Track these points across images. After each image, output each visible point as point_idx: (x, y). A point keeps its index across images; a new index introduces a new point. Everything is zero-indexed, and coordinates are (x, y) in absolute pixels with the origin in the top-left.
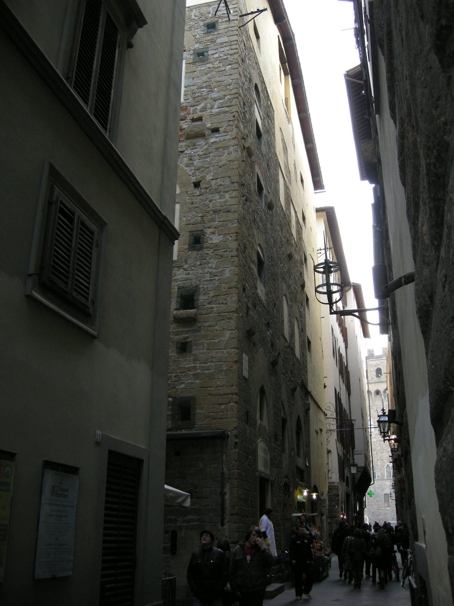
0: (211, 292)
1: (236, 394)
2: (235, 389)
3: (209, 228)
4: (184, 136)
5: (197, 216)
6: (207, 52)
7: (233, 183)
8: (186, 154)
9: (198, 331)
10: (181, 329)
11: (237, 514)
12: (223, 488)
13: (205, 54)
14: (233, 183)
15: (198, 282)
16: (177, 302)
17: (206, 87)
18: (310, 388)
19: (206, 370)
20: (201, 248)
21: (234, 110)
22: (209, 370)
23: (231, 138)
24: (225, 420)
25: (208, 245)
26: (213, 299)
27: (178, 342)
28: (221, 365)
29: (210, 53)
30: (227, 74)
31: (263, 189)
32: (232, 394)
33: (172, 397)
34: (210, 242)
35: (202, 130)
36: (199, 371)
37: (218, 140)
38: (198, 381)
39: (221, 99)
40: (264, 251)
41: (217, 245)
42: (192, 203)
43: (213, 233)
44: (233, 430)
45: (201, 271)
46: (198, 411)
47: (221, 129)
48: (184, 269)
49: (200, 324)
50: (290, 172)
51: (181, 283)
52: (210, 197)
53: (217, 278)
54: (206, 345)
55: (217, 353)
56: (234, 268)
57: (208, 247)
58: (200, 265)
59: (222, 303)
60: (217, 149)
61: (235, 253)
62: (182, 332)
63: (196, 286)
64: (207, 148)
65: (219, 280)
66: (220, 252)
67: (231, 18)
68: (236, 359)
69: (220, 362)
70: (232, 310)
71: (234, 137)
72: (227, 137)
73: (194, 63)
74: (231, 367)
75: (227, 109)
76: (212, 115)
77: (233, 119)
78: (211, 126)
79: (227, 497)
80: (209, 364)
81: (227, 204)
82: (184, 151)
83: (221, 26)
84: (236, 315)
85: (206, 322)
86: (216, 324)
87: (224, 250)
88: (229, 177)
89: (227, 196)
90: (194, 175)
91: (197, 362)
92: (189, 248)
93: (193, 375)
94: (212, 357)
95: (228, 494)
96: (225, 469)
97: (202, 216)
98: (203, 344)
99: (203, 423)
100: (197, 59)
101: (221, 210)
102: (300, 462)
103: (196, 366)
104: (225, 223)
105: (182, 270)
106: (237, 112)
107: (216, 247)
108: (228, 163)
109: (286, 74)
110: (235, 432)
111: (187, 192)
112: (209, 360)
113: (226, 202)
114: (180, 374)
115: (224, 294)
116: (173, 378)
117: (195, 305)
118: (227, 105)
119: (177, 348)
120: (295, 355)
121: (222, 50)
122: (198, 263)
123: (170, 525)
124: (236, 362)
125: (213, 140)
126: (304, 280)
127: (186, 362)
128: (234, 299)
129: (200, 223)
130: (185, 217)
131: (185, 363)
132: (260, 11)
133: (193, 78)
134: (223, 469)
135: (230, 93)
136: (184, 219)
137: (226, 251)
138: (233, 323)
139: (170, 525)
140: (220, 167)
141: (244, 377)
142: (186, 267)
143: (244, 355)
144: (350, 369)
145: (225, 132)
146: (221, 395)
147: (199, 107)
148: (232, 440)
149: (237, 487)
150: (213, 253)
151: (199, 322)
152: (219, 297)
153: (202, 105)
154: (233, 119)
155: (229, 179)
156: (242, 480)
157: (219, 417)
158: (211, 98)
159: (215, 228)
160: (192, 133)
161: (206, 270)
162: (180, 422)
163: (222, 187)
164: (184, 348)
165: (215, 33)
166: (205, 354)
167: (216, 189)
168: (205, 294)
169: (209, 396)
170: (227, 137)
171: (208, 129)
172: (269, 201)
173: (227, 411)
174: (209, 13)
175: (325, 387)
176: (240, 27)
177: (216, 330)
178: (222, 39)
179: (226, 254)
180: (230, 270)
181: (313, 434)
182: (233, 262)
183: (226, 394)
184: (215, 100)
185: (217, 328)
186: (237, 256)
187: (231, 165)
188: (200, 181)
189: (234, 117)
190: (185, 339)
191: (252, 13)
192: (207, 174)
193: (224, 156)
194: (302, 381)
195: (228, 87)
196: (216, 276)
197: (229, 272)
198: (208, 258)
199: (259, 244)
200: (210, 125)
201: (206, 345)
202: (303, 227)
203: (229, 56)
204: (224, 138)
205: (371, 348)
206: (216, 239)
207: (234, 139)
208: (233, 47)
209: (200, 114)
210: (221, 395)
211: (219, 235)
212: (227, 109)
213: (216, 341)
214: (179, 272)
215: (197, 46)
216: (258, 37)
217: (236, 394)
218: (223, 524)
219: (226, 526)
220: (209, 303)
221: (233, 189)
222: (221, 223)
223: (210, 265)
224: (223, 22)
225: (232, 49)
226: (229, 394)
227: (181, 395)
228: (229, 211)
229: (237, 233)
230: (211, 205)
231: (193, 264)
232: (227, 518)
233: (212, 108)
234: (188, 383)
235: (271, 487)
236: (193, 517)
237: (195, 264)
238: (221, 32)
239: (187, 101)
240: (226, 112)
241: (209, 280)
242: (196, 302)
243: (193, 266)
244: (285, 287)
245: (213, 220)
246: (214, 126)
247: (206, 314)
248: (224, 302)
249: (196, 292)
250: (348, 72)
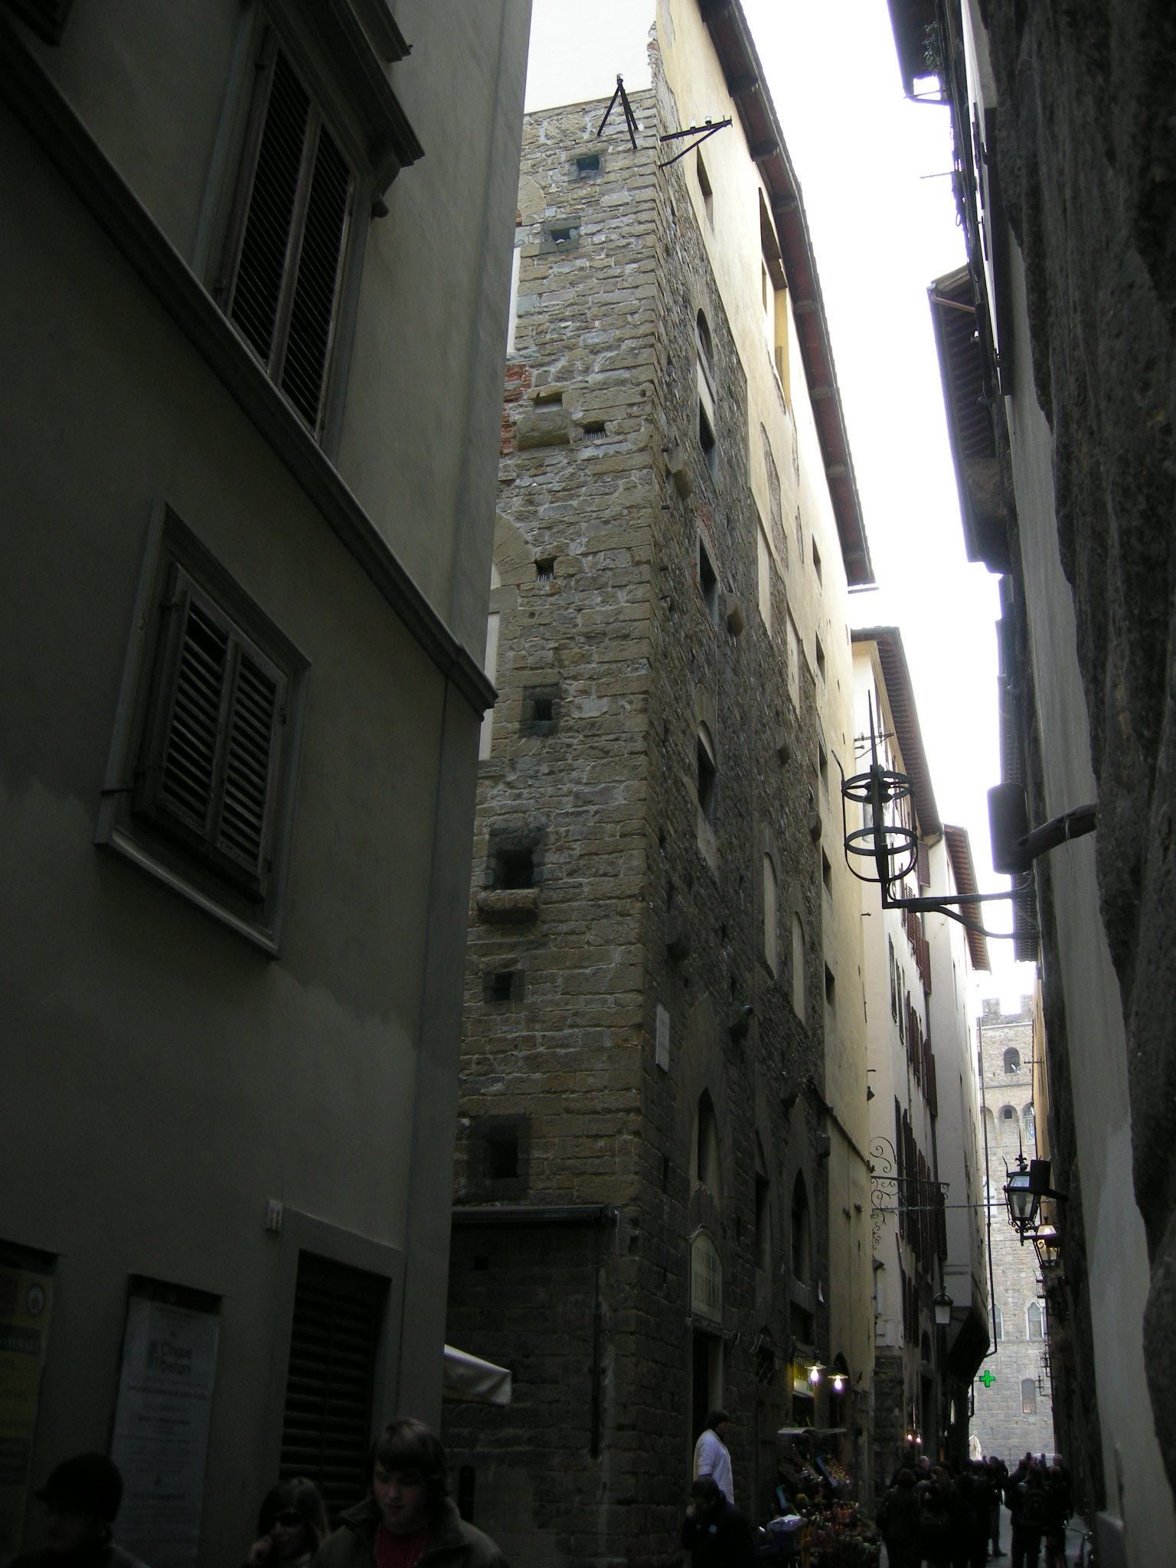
0: (576, 845)
1: (638, 1111)
2: (633, 1098)
3: (574, 678)
4: (514, 443)
5: (543, 648)
6: (576, 228)
7: (638, 564)
8: (519, 487)
9: (543, 945)
10: (497, 940)
11: (634, 1428)
12: (598, 1354)
13: (573, 233)
14: (638, 564)
15: (544, 819)
16: (488, 868)
17: (573, 318)
18: (831, 1098)
19: (562, 1046)
20: (553, 731)
21: (643, 378)
22: (568, 1046)
23: (635, 448)
24: (606, 1178)
25: (571, 722)
26: (582, 862)
27: (487, 974)
28: (600, 1034)
29: (583, 230)
30: (626, 285)
31: (715, 579)
32: (628, 1111)
33: (470, 1117)
34: (576, 715)
35: (560, 429)
36: (541, 1049)
37: (600, 453)
38: (538, 1075)
39: (610, 348)
40: (716, 740)
41: (593, 724)
42: (532, 615)
43: (585, 692)
44: (626, 1205)
45: (550, 790)
46: (537, 1154)
47: (608, 426)
48: (509, 785)
49: (546, 927)
50: (785, 537)
51: (498, 821)
52: (577, 598)
53: (593, 808)
54: (560, 981)
55: (588, 1003)
56: (636, 783)
57: (570, 729)
58: (551, 773)
59: (605, 875)
60: (598, 476)
61: (639, 745)
62: (500, 945)
63: (539, 829)
64: (572, 474)
65: (597, 812)
66: (602, 742)
67: (639, 142)
68: (638, 1020)
69: (597, 1026)
70: (629, 893)
71: (642, 445)
72: (624, 447)
73: (541, 256)
74: (626, 1041)
75: (626, 375)
76: (587, 389)
77: (639, 399)
78: (583, 418)
79: (608, 1381)
80: (567, 1031)
81: (621, 617)
82: (513, 480)
83: (615, 164)
84: (639, 904)
85: (561, 922)
86: (589, 928)
87: (612, 737)
88: (629, 549)
89: (622, 596)
90: (537, 542)
91: (537, 1026)
92: (520, 730)
93: (527, 1058)
94: (576, 1014)
95: (610, 1373)
96: (605, 1308)
97: (556, 649)
98: (553, 979)
99: (548, 1184)
100: (551, 246)
101: (605, 634)
102: (802, 1291)
103: (534, 1036)
104: (614, 666)
105: (501, 786)
106: (652, 382)
107: (591, 728)
108: (625, 512)
109: (778, 287)
110: (632, 1211)
111: (518, 586)
112: (569, 1021)
113: (619, 612)
114: (491, 1057)
115: (610, 849)
116: (474, 1066)
117: (536, 877)
118: (625, 363)
119: (485, 988)
120: (792, 1011)
121: (615, 223)
122: (545, 769)
123: (456, 1450)
124: (639, 1027)
125: (587, 453)
126: (818, 816)
127: (509, 1026)
128: (635, 863)
129: (553, 666)
130: (512, 649)
131: (505, 1028)
132: (712, 127)
133: (540, 295)
134: (598, 1305)
135: (634, 332)
136: (511, 654)
137: (617, 739)
138: (631, 927)
139: (456, 1450)
140: (606, 522)
142: (511, 777)
143: (660, 1009)
144: (934, 1051)
145: (619, 434)
146: (598, 1113)
147: (553, 369)
148: (623, 1232)
149: (633, 1355)
150: (582, 742)
151: (545, 922)
152: (597, 858)
153: (562, 363)
154: (639, 399)
155: (628, 555)
158: (586, 347)
159: (591, 678)
160: (536, 434)
161: (565, 789)
162: (488, 1182)
163: (610, 573)
164: (503, 988)
165: (599, 181)
166: (558, 1004)
167: (594, 579)
168: (560, 849)
169: (565, 1116)
170: (624, 447)
171: (577, 424)
172: (729, 612)
174: (584, 129)
175: (870, 1095)
176: (661, 166)
177: (588, 943)
178: (615, 196)
179: (616, 745)
180: (627, 789)
181: (836, 1219)
182: (635, 768)
183: (609, 1111)
184: (595, 351)
185: (589, 937)
186: (645, 753)
187: (633, 519)
188: (555, 558)
189: (643, 394)
190: (506, 966)
191: (694, 130)
192: (572, 540)
193: (616, 494)
194: (810, 1080)
195: (629, 318)
196: (590, 802)
197: (625, 793)
198: (570, 757)
199: (703, 723)
200: (581, 414)
201: (560, 981)
202: (818, 681)
203: (632, 240)
204: (617, 447)
205: (991, 996)
206: (592, 708)
207: (642, 450)
208: (644, 216)
209: (555, 386)
210: (598, 1113)
211: (599, 697)
212: (626, 375)
213: (588, 971)
214: (495, 792)
215: (550, 213)
216: (707, 191)
217: (638, 1111)
218: (595, 1452)
219: (605, 1458)
220: (570, 874)
221: (638, 578)
222: (606, 666)
223: (574, 774)
224: (619, 153)
225: (640, 223)
226: (618, 1111)
227: (493, 1112)
228: (625, 637)
229: (646, 692)
230: (579, 621)
231: (531, 772)
232: (607, 1436)
233: (587, 370)
234: (511, 1081)
235: (725, 1356)
236: (520, 1432)
237: (537, 771)
238: (612, 177)
239: (522, 352)
240: (623, 382)
241: (572, 813)
242: (536, 870)
243: (531, 777)
244: (768, 833)
245: (585, 658)
246: (593, 417)
247: (562, 901)
248: (609, 869)
249: (538, 843)
250: (938, 282)
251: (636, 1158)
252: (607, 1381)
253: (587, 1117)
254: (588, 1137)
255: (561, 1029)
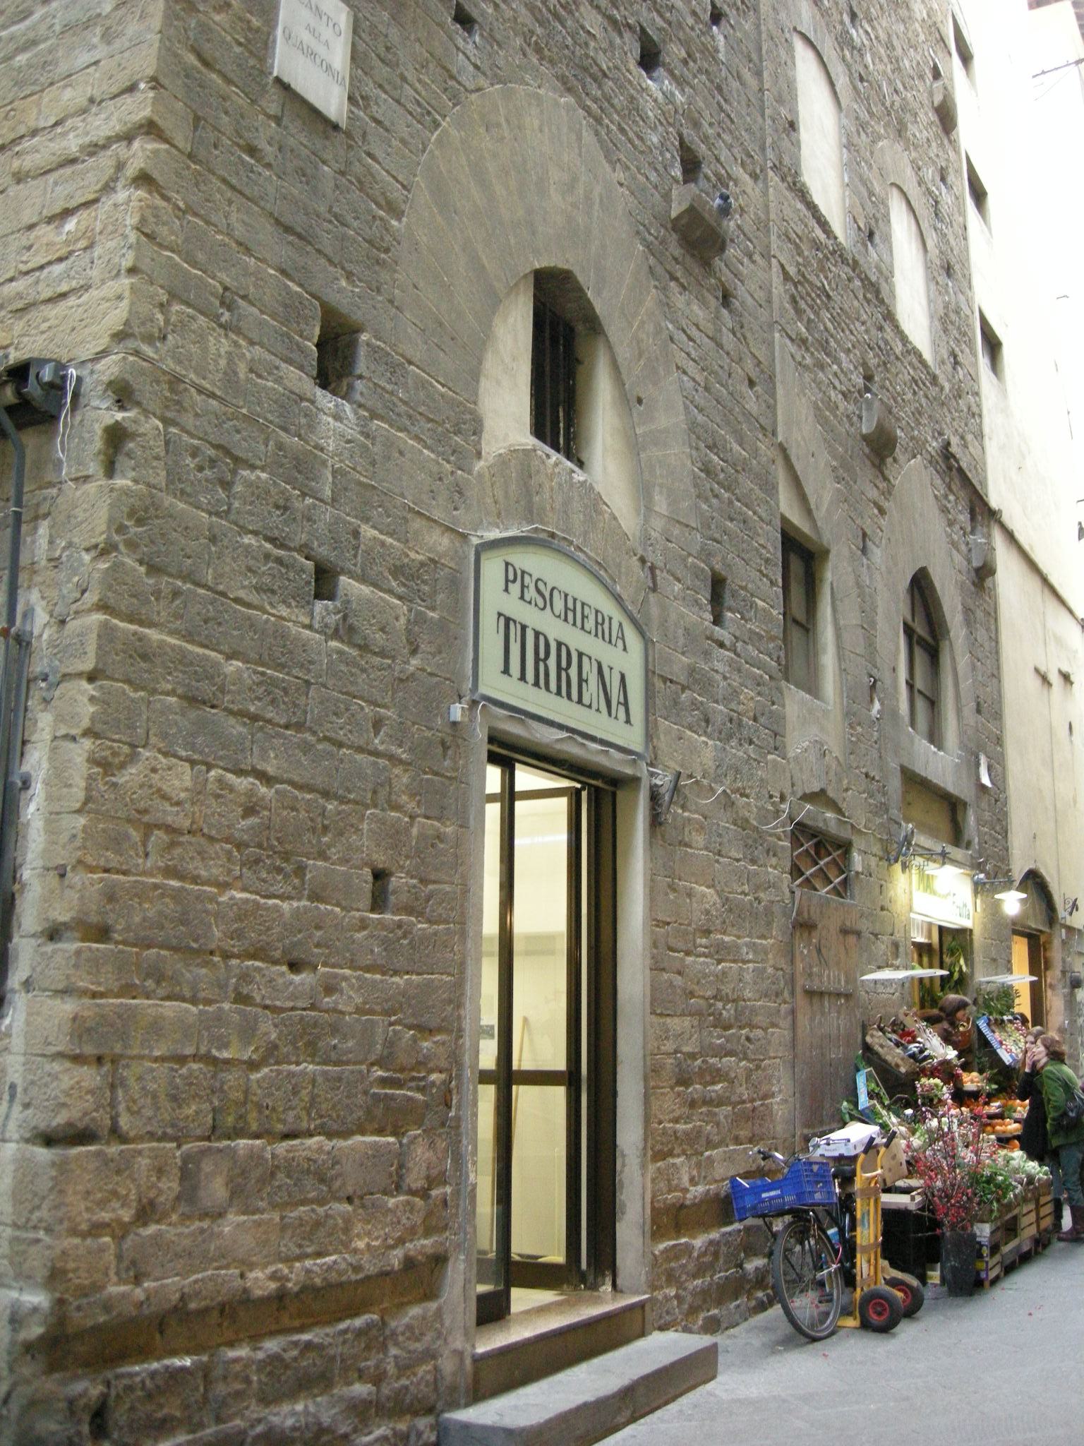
1: (150, 128)
22: (34, 43)
24: (72, 301)
32: (128, 138)
44: (103, 354)
95: (38, 788)
110: (110, 368)
141: (278, 80)
146: (73, 161)
149: (87, 733)
156: (193, 700)
157: (47, 294)
173: (90, 246)
210: (73, 161)
251: (133, 237)
252: (32, 808)
253: (51, 178)
254: (50, 220)
255: (31, 14)
